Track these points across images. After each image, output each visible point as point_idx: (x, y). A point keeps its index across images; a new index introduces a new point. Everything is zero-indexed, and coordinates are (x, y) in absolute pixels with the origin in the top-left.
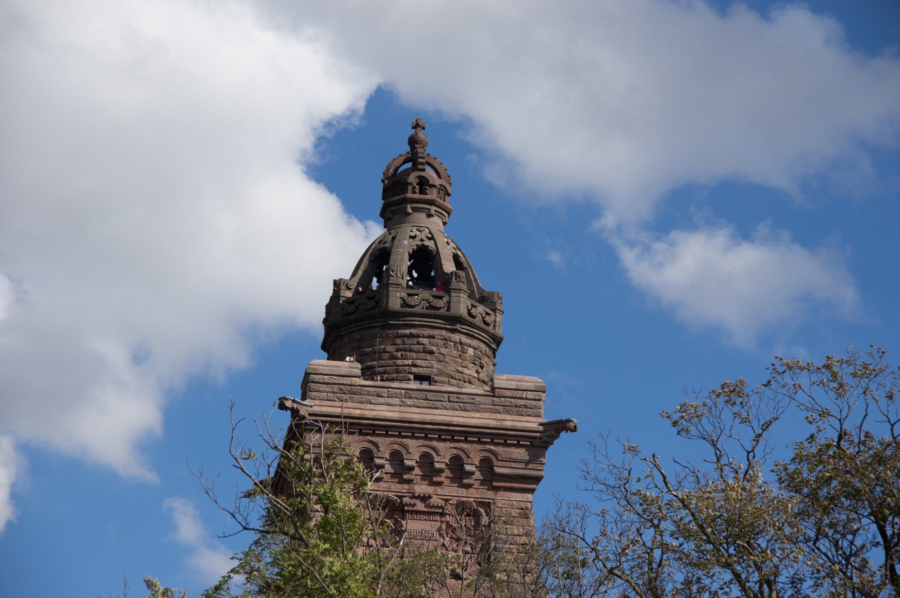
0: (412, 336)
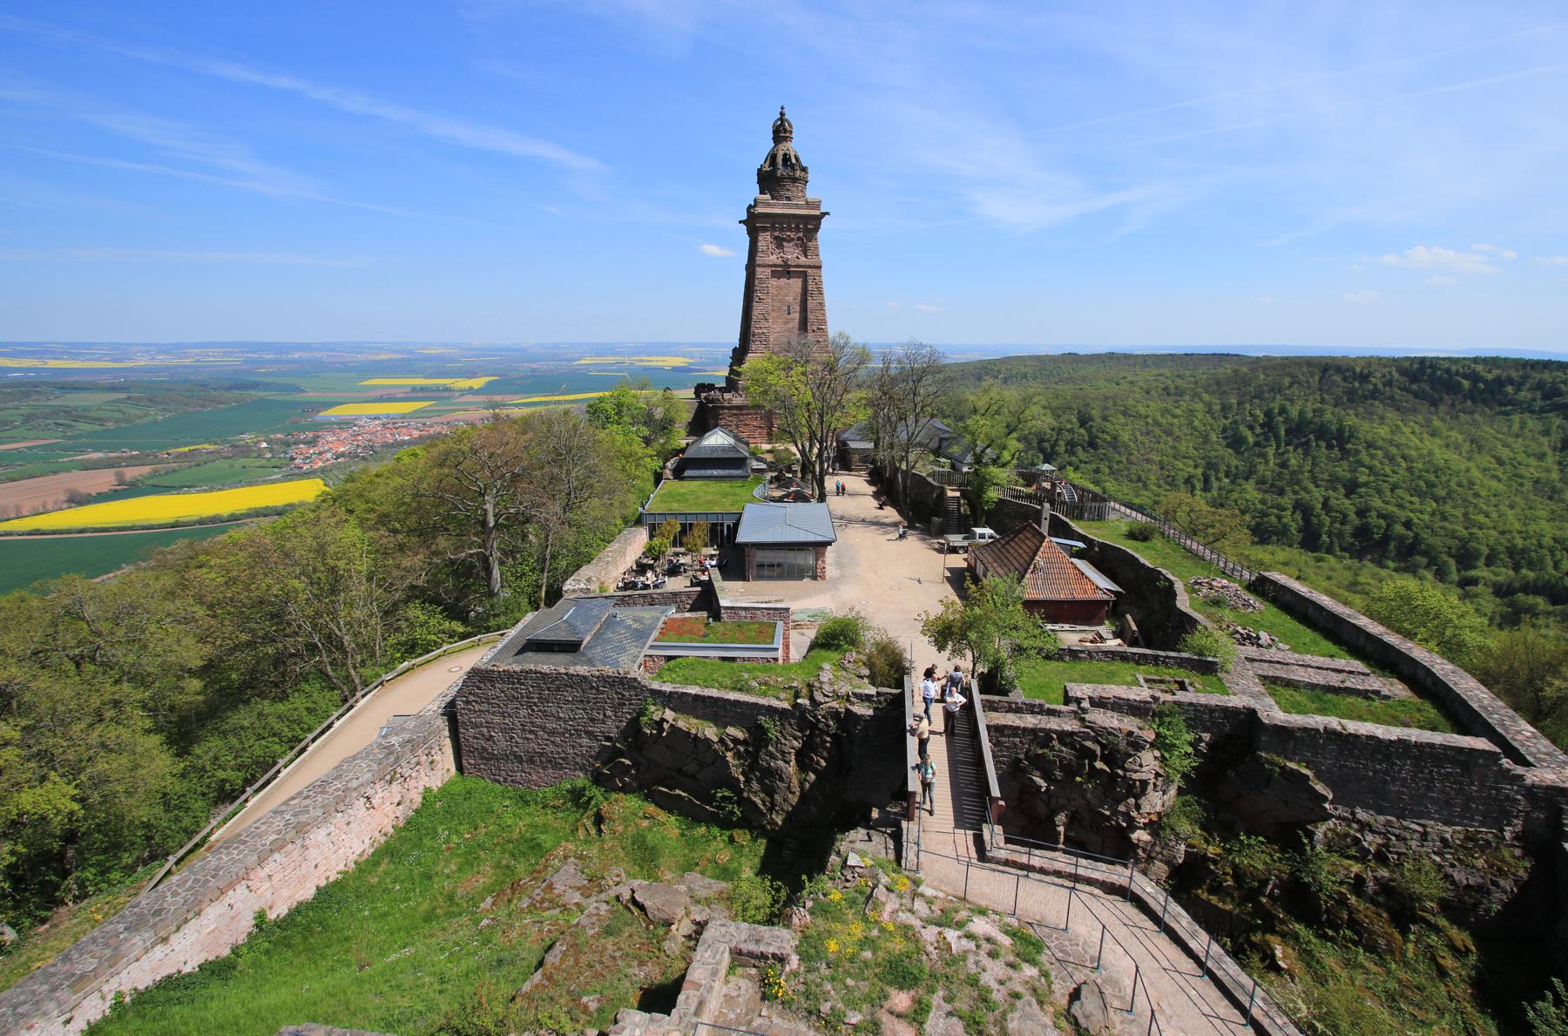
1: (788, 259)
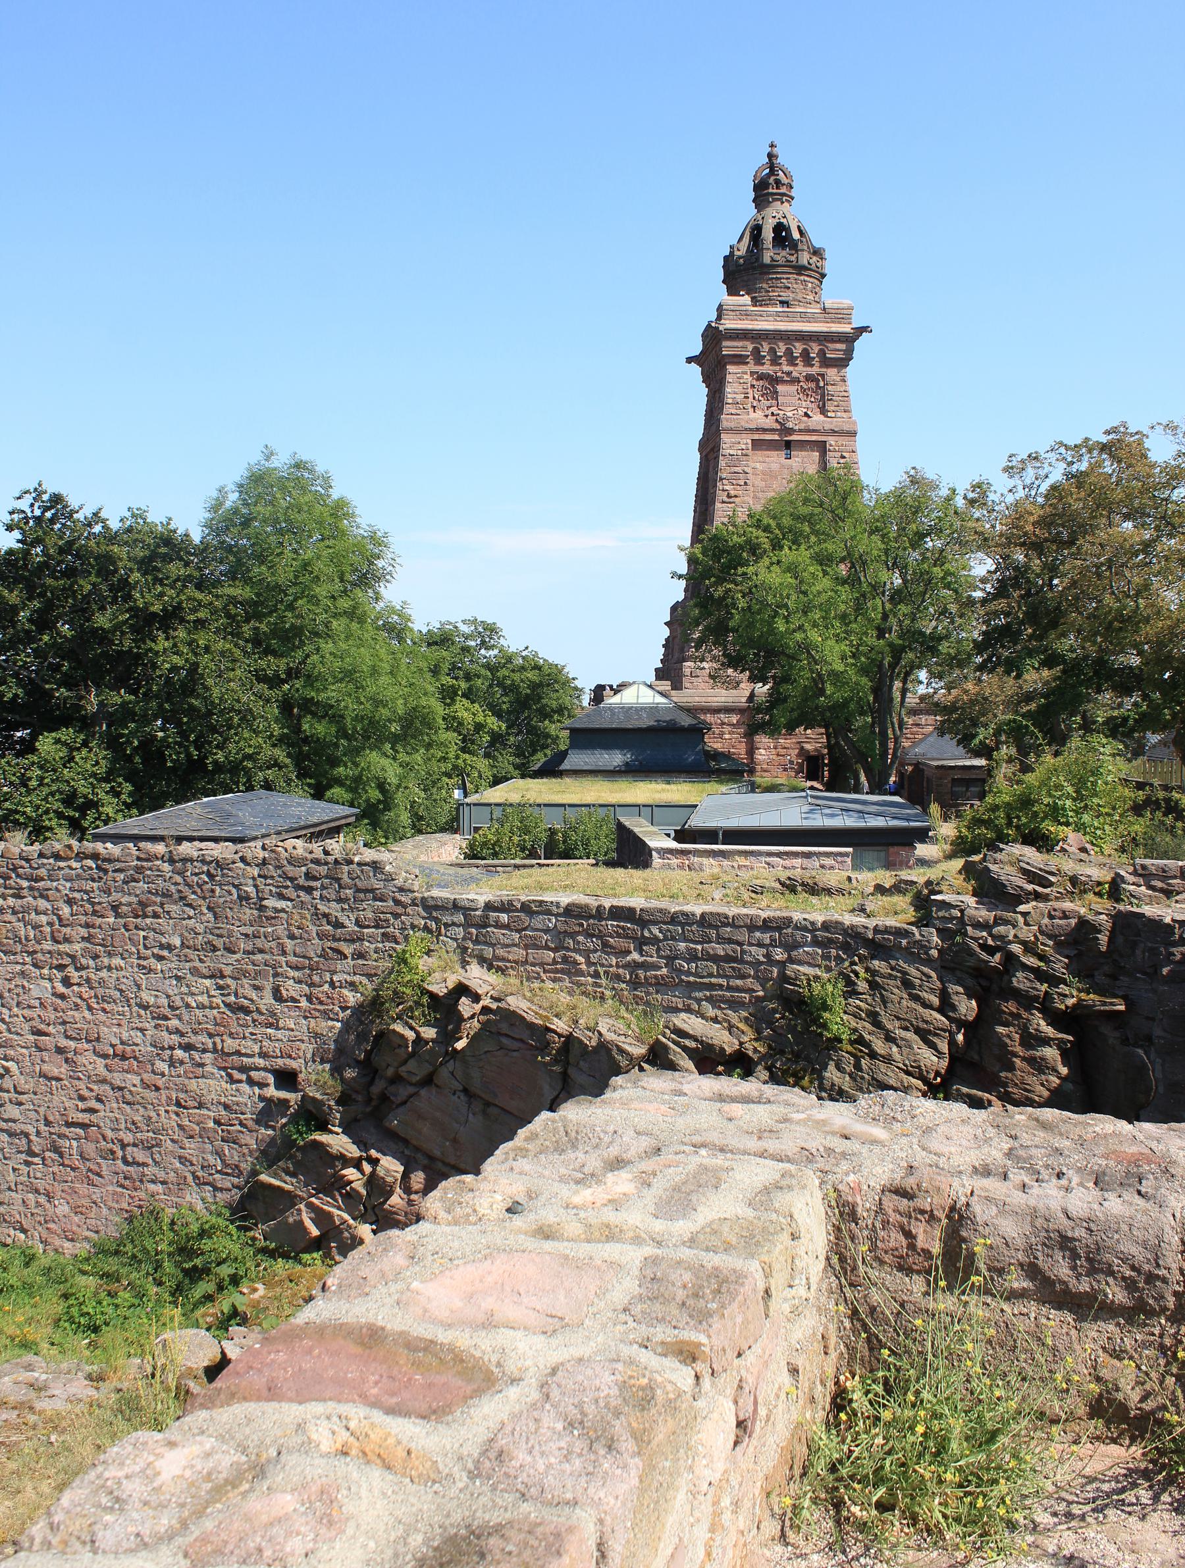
0: (777, 279)
1: (787, 419)
